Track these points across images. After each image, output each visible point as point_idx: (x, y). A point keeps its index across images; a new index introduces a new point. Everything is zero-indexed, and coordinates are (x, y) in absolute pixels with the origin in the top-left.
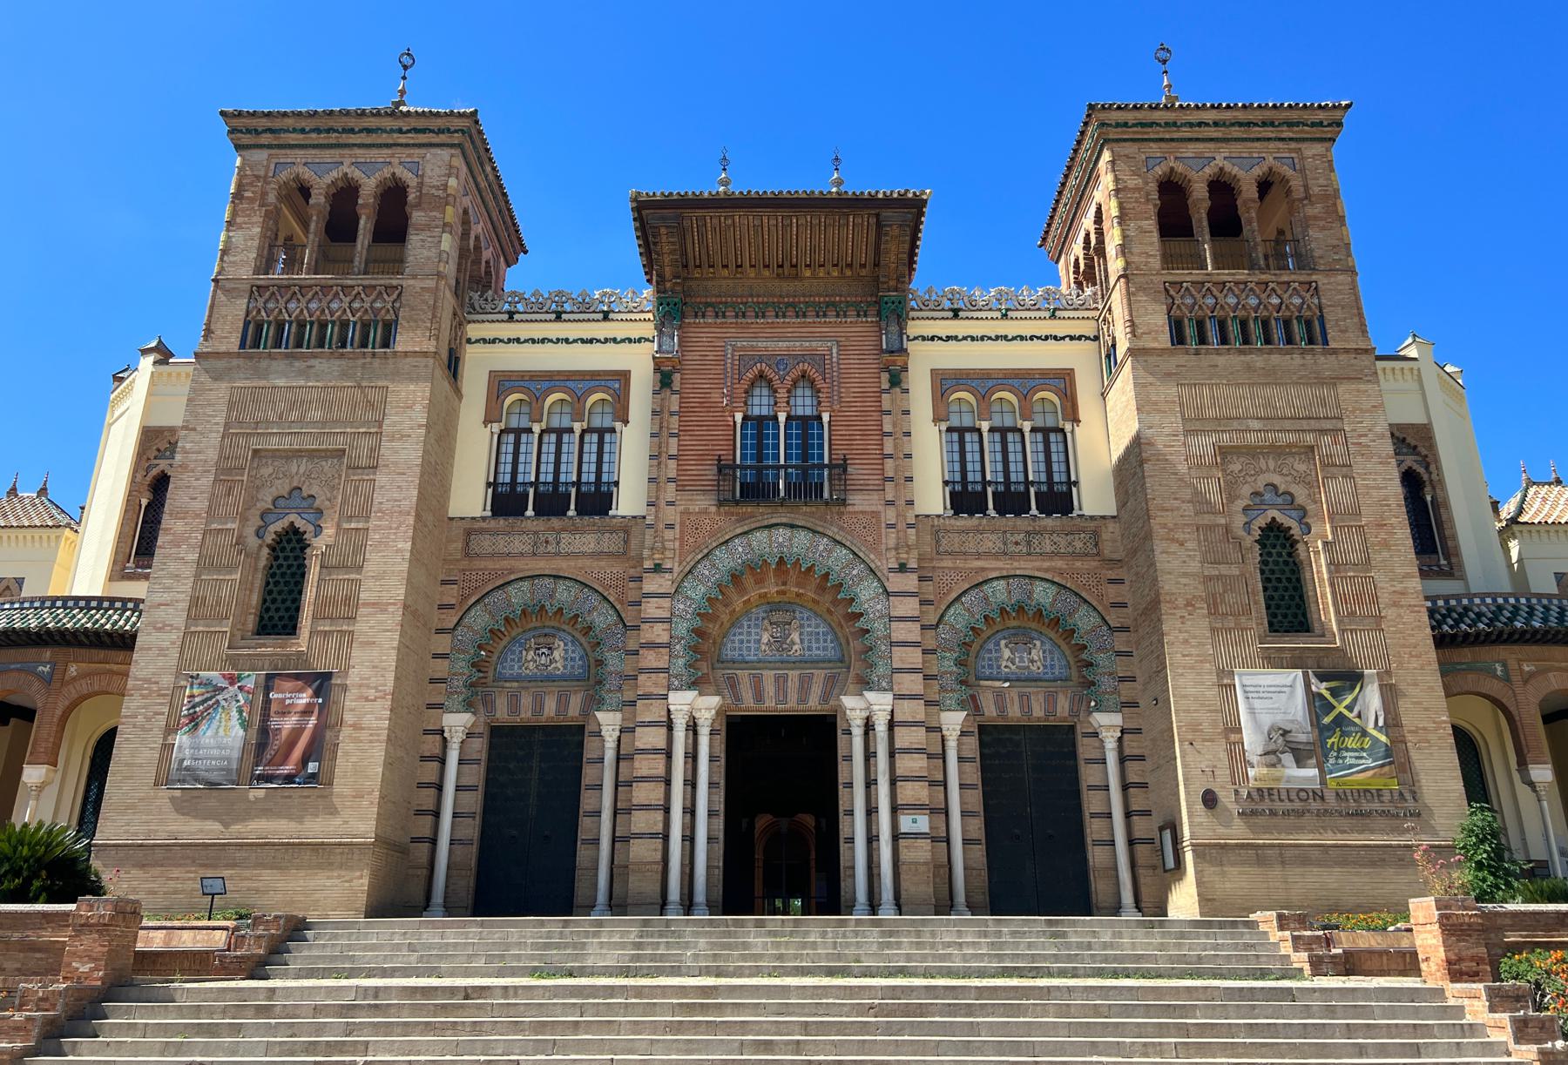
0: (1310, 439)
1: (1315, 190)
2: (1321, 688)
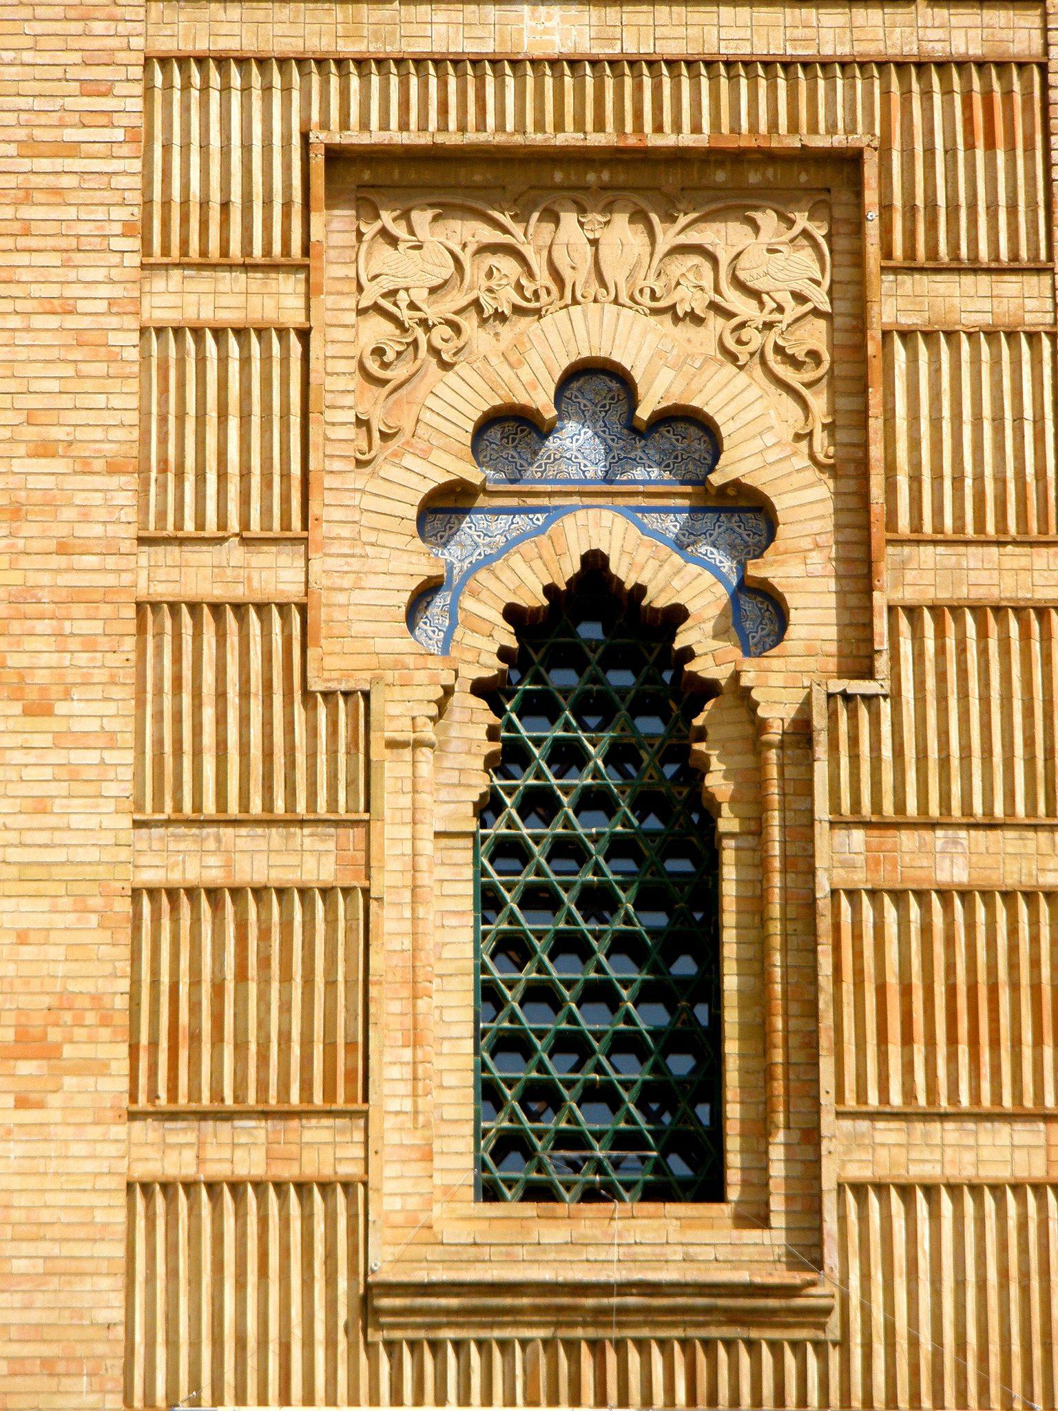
0: (837, 119)
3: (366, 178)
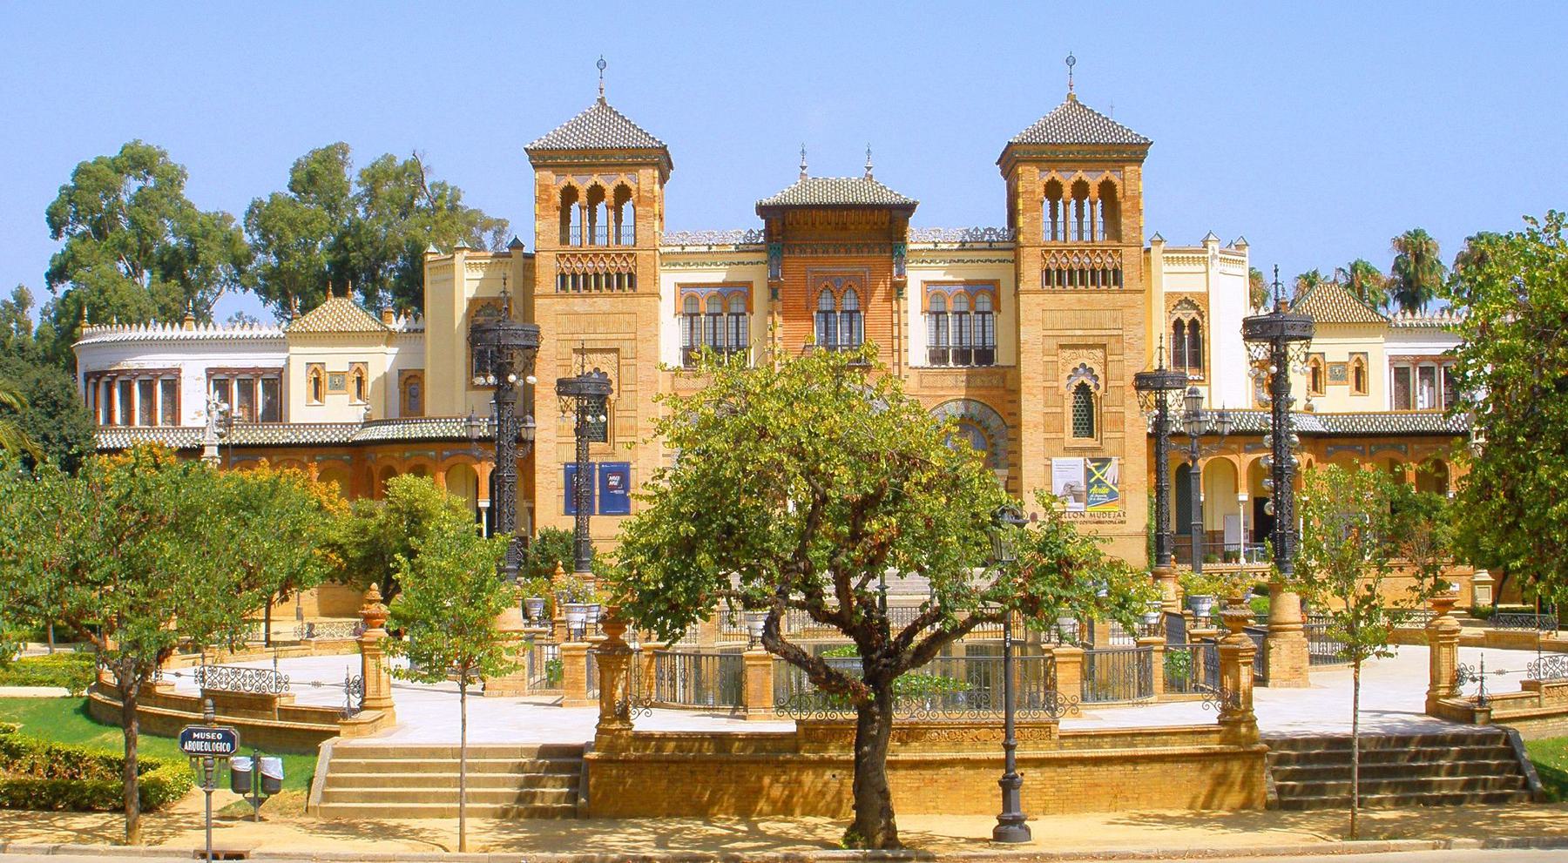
1: (1129, 193)
2: (1091, 466)
3: (1062, 347)
